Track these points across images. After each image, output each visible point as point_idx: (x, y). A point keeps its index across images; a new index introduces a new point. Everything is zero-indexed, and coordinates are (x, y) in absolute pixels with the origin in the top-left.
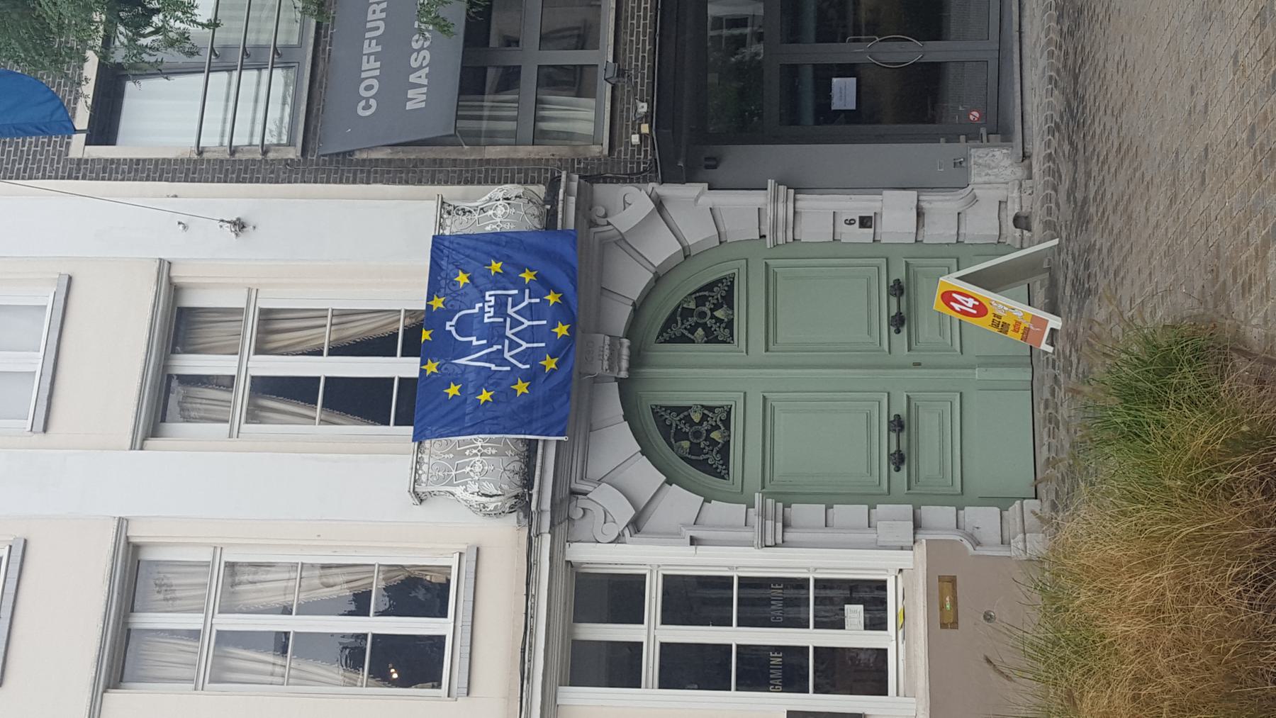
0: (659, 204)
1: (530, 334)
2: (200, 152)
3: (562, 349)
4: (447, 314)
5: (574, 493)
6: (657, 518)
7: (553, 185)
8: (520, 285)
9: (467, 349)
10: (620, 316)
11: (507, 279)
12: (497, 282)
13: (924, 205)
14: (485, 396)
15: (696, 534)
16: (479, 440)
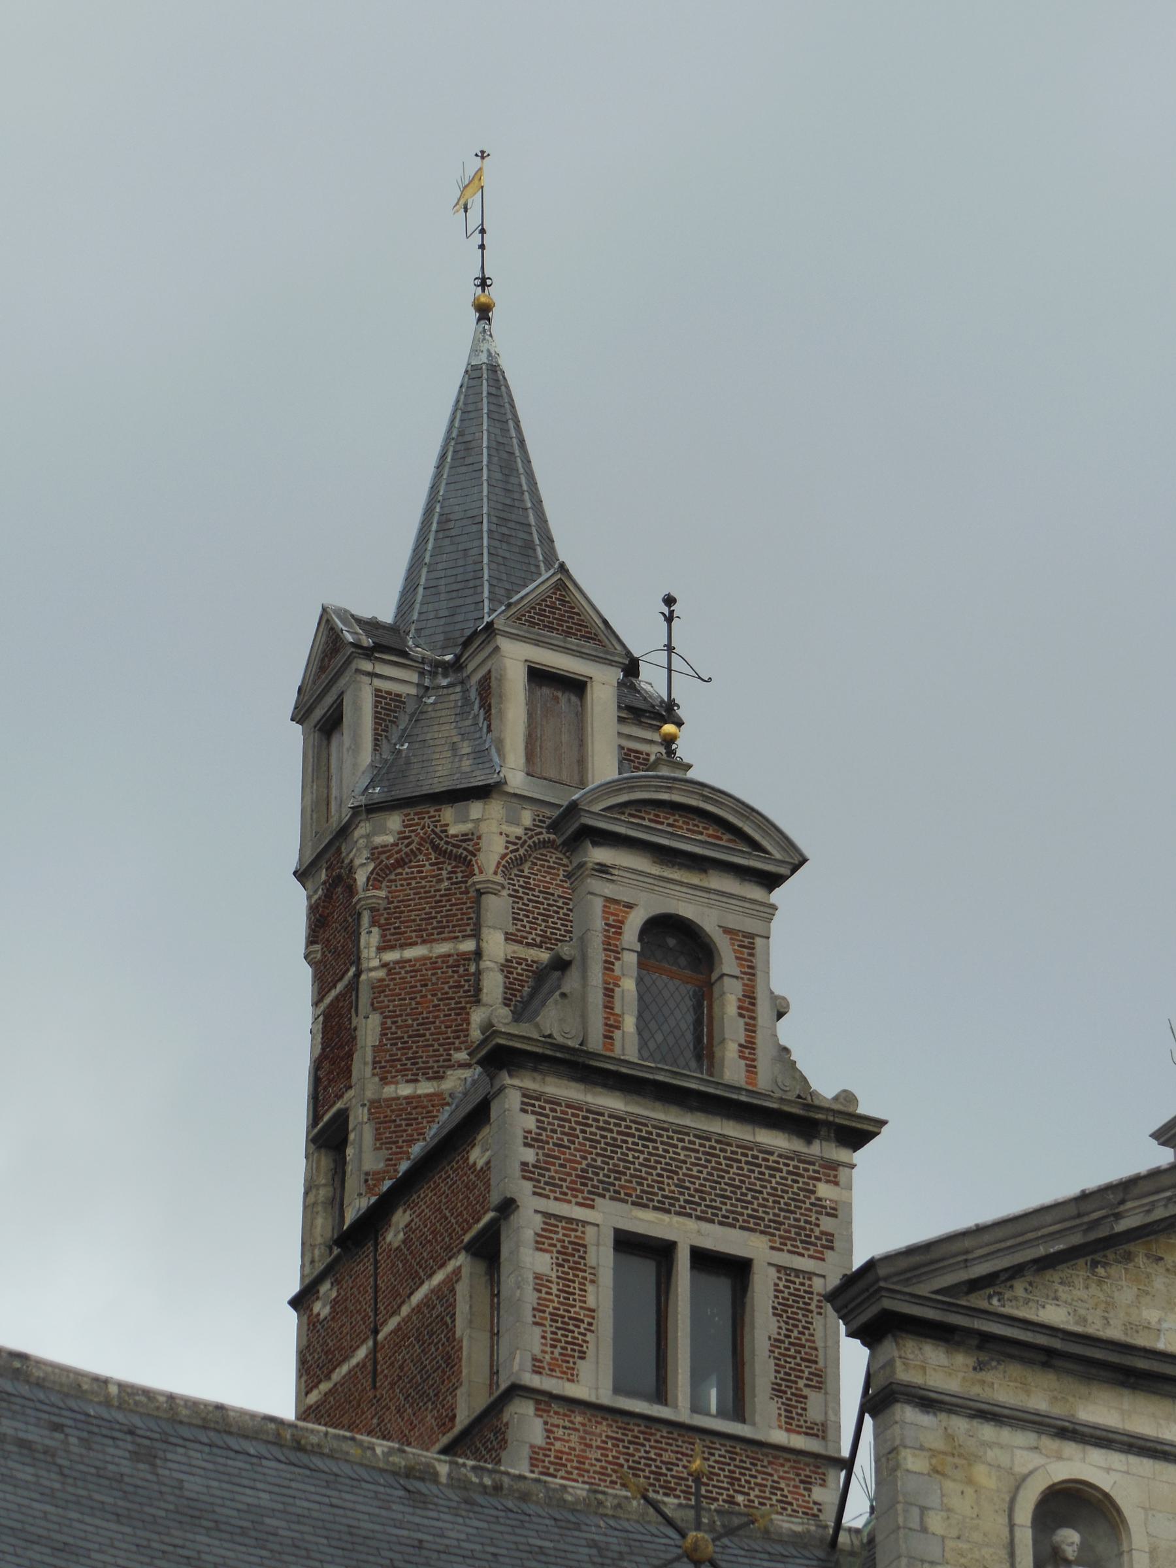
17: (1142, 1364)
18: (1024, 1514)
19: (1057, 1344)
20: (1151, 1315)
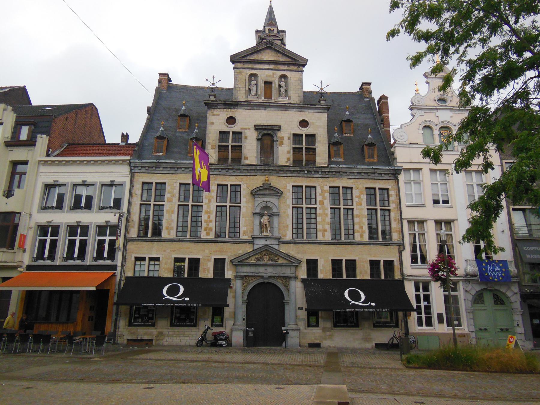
0: (516, 293)
1: (494, 275)
2: (513, 224)
3: (493, 280)
4: (495, 263)
5: (469, 282)
6: (468, 295)
7: (517, 277)
8: (502, 273)
9: (490, 266)
10: (497, 288)
11: (502, 272)
12: (502, 271)
13: (522, 334)
14: (484, 269)
15: (466, 300)
16: (477, 269)
17: (260, 61)
18: (247, 77)
19: (251, 61)
20: (263, 57)
